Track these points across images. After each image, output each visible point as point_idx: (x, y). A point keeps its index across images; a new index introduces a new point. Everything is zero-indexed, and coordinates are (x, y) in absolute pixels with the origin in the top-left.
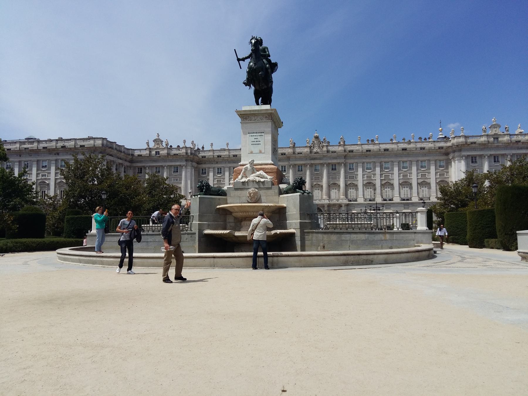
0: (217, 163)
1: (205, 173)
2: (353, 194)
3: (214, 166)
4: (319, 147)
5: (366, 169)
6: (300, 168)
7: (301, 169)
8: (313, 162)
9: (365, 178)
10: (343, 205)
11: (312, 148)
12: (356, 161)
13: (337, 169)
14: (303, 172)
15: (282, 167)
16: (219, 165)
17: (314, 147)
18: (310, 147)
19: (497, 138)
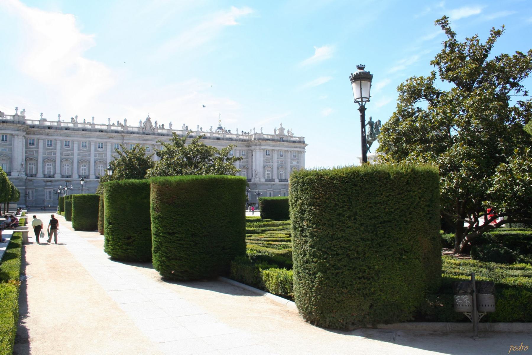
0: (48, 134)
3: (44, 137)
8: (145, 142)
16: (50, 138)
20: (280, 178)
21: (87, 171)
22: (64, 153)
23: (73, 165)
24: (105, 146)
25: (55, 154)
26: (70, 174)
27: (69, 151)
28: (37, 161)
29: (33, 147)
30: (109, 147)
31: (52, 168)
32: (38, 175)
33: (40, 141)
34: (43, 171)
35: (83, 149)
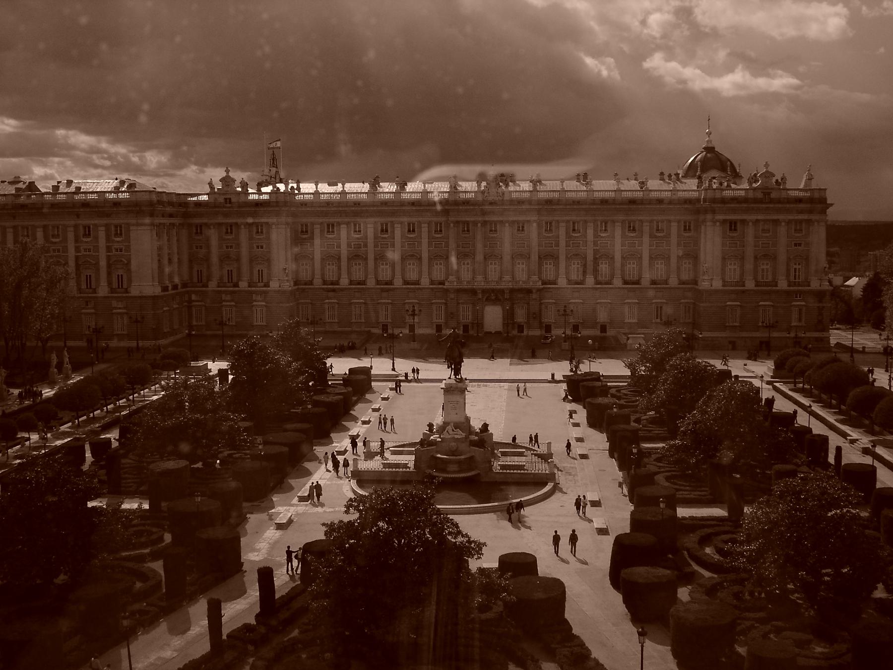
1: (307, 232)
2: (387, 272)
4: (497, 192)
5: (571, 232)
6: (119, 229)
7: (358, 228)
9: (378, 248)
10: (534, 291)
11: (486, 194)
12: (556, 218)
13: (443, 231)
14: (471, 234)
15: (302, 225)
17: (489, 193)
18: (483, 192)
19: (769, 194)
20: (792, 279)
21: (389, 272)
22: (352, 243)
23: (367, 264)
24: (417, 228)
25: (339, 246)
26: (362, 278)
27: (361, 241)
28: (313, 259)
29: (306, 236)
30: (425, 229)
31: (335, 268)
32: (315, 281)
33: (315, 226)
34: (323, 275)
35: (382, 236)
